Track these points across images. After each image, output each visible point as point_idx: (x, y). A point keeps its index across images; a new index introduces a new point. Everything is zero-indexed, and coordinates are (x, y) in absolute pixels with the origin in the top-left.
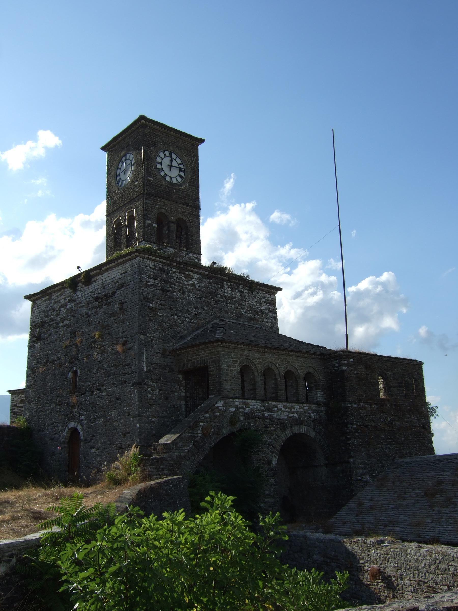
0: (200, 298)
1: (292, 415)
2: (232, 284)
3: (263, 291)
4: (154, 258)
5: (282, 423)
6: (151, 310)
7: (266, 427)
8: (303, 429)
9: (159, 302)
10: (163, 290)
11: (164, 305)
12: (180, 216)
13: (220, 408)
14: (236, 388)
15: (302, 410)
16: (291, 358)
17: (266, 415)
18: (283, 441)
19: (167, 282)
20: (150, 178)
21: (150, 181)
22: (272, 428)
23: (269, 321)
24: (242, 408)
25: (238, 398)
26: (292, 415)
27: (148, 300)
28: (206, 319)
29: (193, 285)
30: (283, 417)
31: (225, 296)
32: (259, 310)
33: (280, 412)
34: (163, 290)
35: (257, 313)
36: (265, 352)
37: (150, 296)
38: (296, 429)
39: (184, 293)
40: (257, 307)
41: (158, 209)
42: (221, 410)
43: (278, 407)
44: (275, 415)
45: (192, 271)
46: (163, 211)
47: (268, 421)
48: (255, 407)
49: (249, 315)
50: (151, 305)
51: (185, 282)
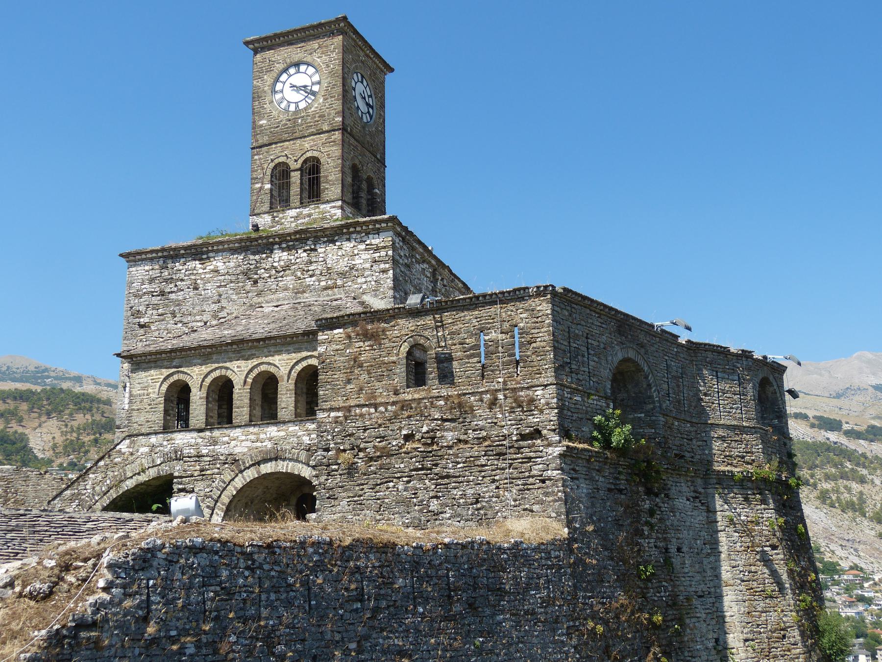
0: (225, 286)
1: (259, 444)
2: (291, 243)
3: (359, 232)
4: (149, 256)
5: (235, 460)
6: (142, 326)
7: (202, 471)
8: (282, 467)
9: (155, 312)
10: (162, 293)
11: (162, 315)
12: (309, 154)
13: (123, 451)
14: (153, 419)
15: (282, 434)
16: (265, 350)
17: (204, 452)
18: (235, 488)
19: (168, 281)
20: (261, 122)
21: (261, 126)
22: (216, 471)
23: (369, 279)
24: (161, 445)
25: (156, 433)
26: (259, 444)
27: (137, 314)
28: (232, 313)
29: (216, 271)
30: (237, 450)
31: (275, 268)
32: (347, 269)
33: (233, 443)
34: (162, 293)
35: (343, 275)
36: (210, 354)
37: (142, 308)
38: (267, 468)
39: (196, 288)
40: (343, 265)
41: (272, 161)
42: (124, 454)
43: (232, 435)
44: (220, 449)
45: (212, 251)
46: (281, 159)
47: (208, 459)
48: (185, 441)
49: (323, 284)
50: (142, 320)
51: (201, 271)
